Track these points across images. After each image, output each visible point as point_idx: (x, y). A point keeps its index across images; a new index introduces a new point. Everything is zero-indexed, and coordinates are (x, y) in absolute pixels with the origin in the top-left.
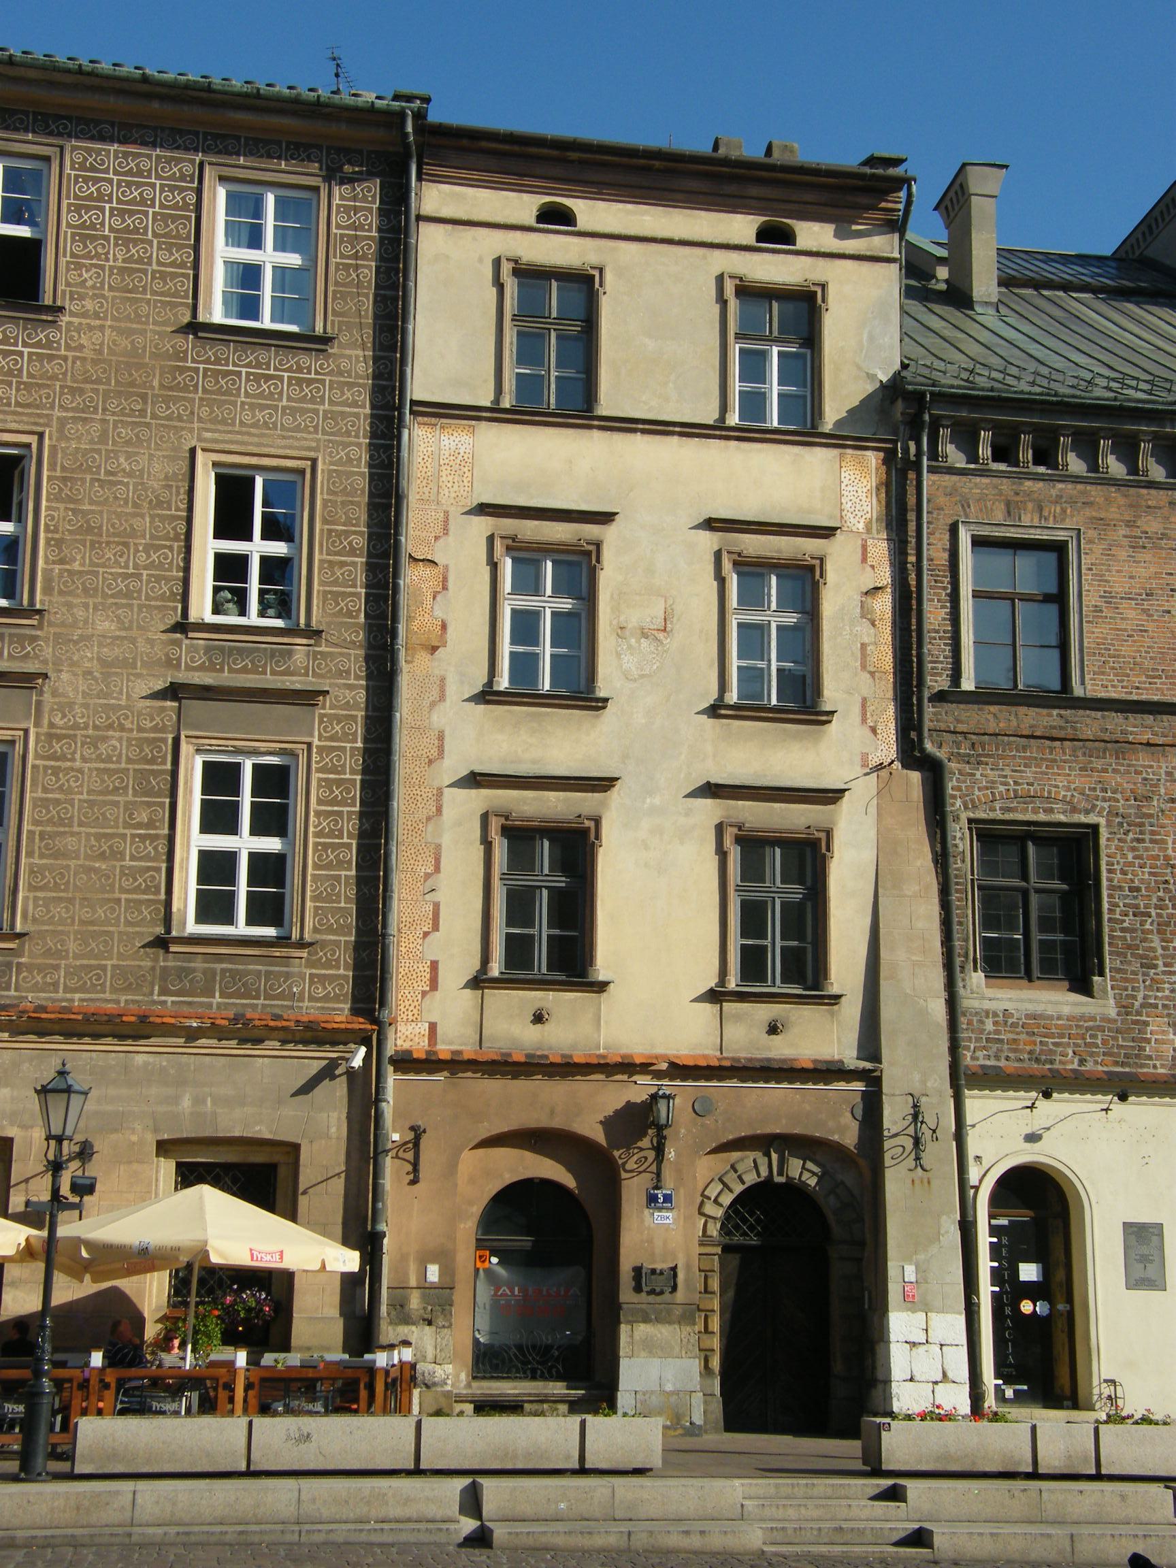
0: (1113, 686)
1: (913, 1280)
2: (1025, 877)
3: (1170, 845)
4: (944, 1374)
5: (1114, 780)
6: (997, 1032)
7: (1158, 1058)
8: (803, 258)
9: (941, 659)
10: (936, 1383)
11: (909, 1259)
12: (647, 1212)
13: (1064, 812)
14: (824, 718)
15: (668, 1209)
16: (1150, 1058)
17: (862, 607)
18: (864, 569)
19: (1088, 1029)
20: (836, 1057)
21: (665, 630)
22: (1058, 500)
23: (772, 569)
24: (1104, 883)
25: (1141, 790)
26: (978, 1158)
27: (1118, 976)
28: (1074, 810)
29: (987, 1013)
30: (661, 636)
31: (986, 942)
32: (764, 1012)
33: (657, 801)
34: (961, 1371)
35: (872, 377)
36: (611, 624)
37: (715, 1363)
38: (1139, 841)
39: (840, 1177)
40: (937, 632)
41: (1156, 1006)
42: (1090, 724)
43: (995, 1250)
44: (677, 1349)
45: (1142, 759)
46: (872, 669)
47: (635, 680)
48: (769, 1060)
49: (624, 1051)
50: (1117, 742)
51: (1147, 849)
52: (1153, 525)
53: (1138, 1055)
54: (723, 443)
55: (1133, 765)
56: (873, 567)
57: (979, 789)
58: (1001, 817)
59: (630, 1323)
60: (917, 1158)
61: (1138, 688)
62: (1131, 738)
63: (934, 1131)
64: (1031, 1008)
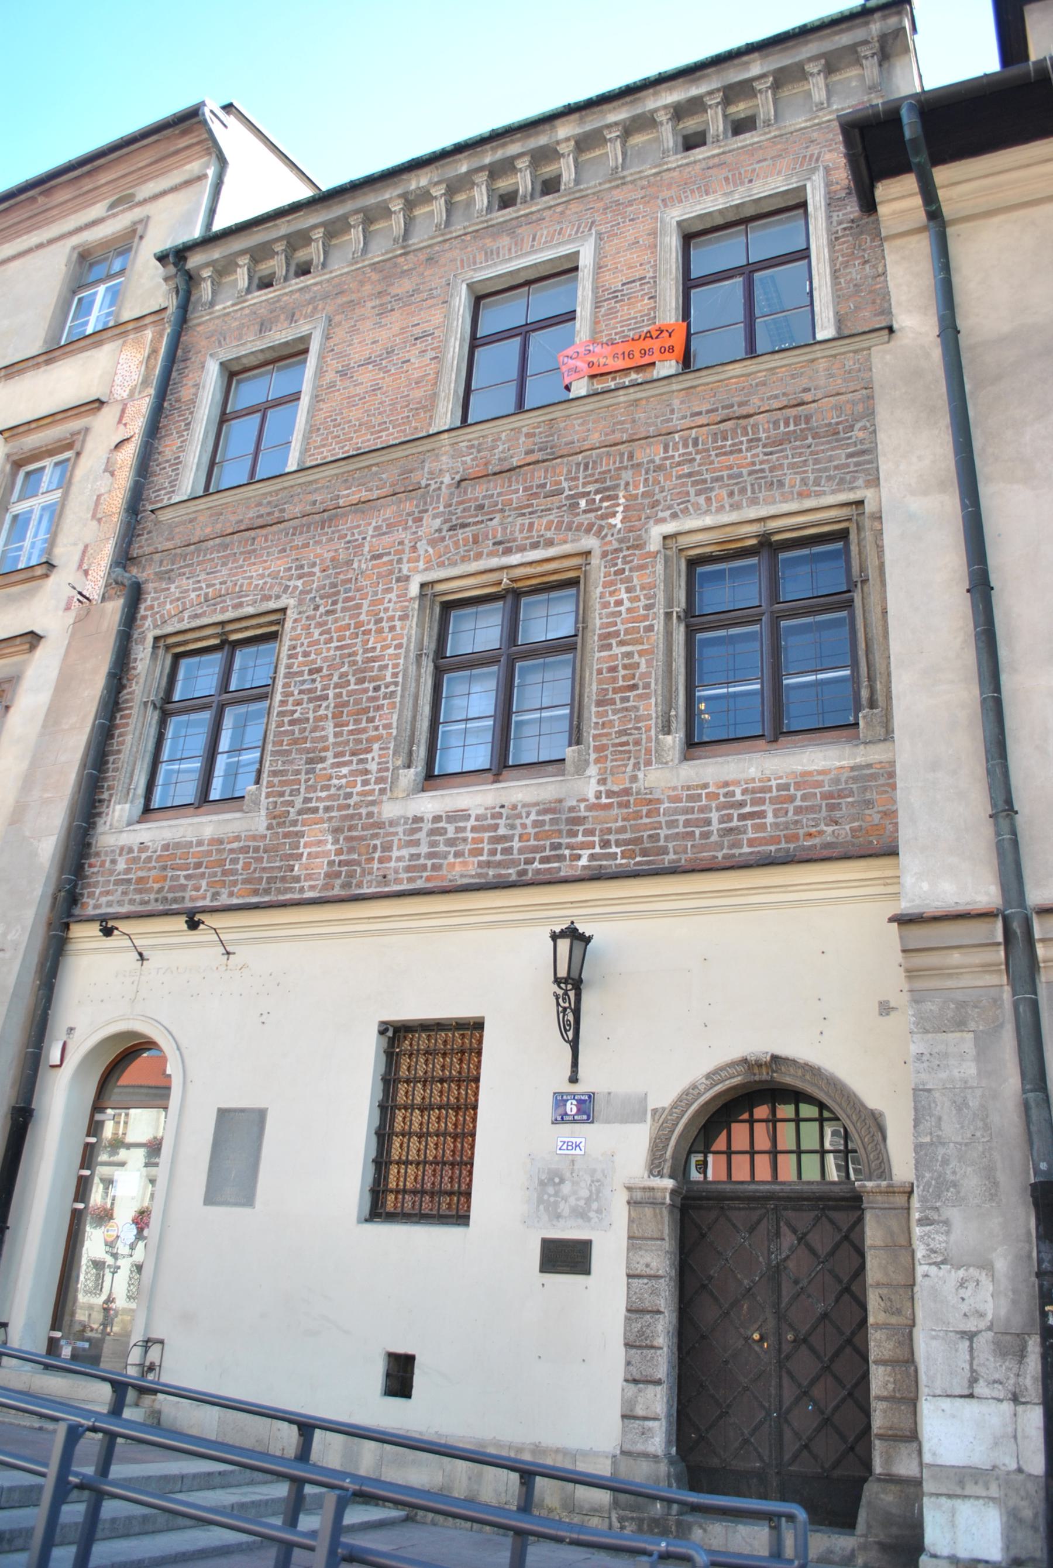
6: (128, 871)
7: (309, 878)
18: (117, 428)
19: (232, 851)
25: (342, 556)
26: (71, 1030)
27: (276, 780)
28: (268, 598)
41: (316, 810)
53: (289, 878)
55: (339, 531)
56: (125, 425)
62: (341, 502)
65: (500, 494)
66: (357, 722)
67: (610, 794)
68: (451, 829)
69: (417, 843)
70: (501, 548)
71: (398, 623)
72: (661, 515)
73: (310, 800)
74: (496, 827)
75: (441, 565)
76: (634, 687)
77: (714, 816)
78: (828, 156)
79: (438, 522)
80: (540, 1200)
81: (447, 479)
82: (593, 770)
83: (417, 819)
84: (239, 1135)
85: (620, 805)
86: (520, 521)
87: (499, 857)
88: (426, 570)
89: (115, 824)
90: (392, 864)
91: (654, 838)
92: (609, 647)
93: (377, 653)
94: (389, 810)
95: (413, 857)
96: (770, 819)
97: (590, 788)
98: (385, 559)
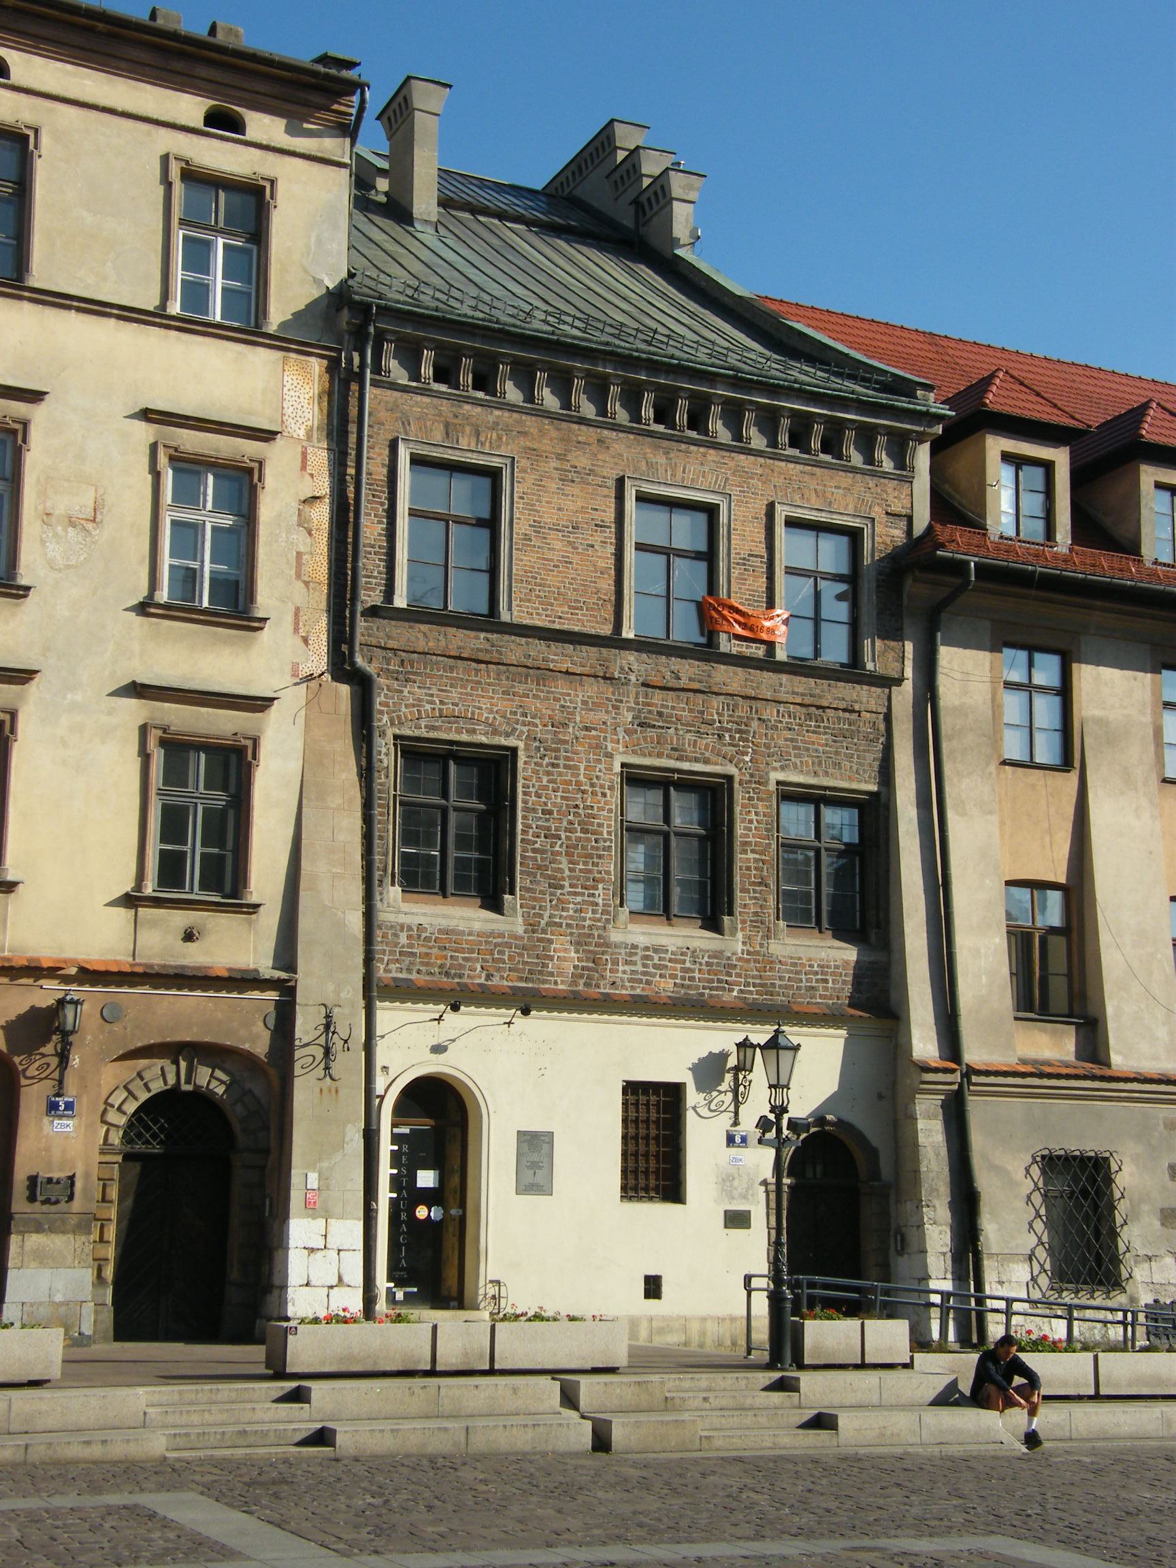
0: (538, 614)
1: (316, 1187)
2: (445, 796)
3: (582, 771)
4: (340, 1279)
5: (533, 705)
6: (411, 946)
8: (252, 150)
9: (376, 574)
10: (331, 1287)
11: (311, 1166)
12: (46, 1120)
13: (486, 734)
14: (256, 625)
15: (68, 1116)
16: (552, 974)
17: (299, 515)
18: (303, 477)
19: (496, 945)
20: (252, 966)
21: (94, 521)
22: (494, 427)
23: (209, 468)
24: (520, 805)
25: (558, 717)
26: (385, 1068)
27: (527, 895)
28: (495, 732)
29: (402, 926)
30: (90, 526)
31: (404, 856)
32: (180, 919)
33: (79, 698)
34: (356, 1276)
35: (318, 282)
36: (36, 509)
37: (109, 1272)
38: (553, 765)
39: (248, 1086)
40: (373, 546)
42: (515, 649)
43: (396, 1158)
44: (70, 1259)
45: (561, 686)
46: (307, 579)
47: (60, 570)
48: (183, 967)
49: (30, 954)
50: (539, 668)
51: (560, 774)
52: (582, 460)
53: (540, 971)
54: (162, 331)
55: (553, 692)
56: (312, 475)
57: (406, 706)
58: (426, 735)
59: (22, 1233)
60: (327, 1068)
61: (560, 618)
62: (551, 666)
63: (346, 1041)
64: (444, 923)
65: (673, 708)
66: (585, 863)
67: (749, 953)
68: (656, 957)
69: (634, 963)
70: (676, 754)
71: (608, 792)
72: (775, 764)
73: (555, 916)
74: (684, 962)
75: (634, 752)
76: (760, 884)
77: (803, 977)
78: (876, 509)
79: (629, 717)
80: (723, 1190)
81: (633, 678)
82: (740, 935)
83: (634, 947)
84: (535, 1149)
85: (756, 961)
86: (688, 736)
87: (687, 982)
88: (624, 753)
89: (391, 901)
90: (620, 975)
91: (773, 985)
92: (745, 852)
93: (595, 812)
94: (615, 936)
95: (633, 972)
96: (830, 985)
97: (739, 947)
98: (593, 733)
